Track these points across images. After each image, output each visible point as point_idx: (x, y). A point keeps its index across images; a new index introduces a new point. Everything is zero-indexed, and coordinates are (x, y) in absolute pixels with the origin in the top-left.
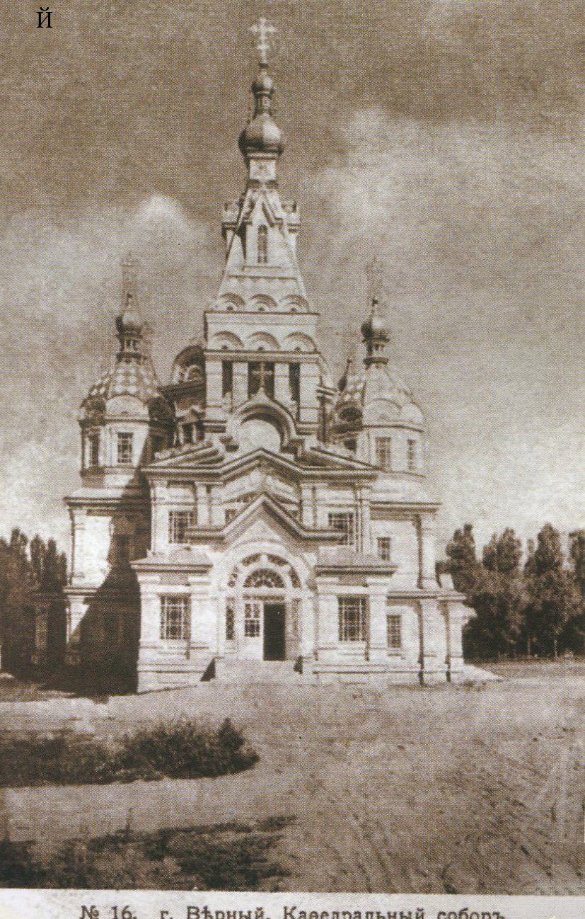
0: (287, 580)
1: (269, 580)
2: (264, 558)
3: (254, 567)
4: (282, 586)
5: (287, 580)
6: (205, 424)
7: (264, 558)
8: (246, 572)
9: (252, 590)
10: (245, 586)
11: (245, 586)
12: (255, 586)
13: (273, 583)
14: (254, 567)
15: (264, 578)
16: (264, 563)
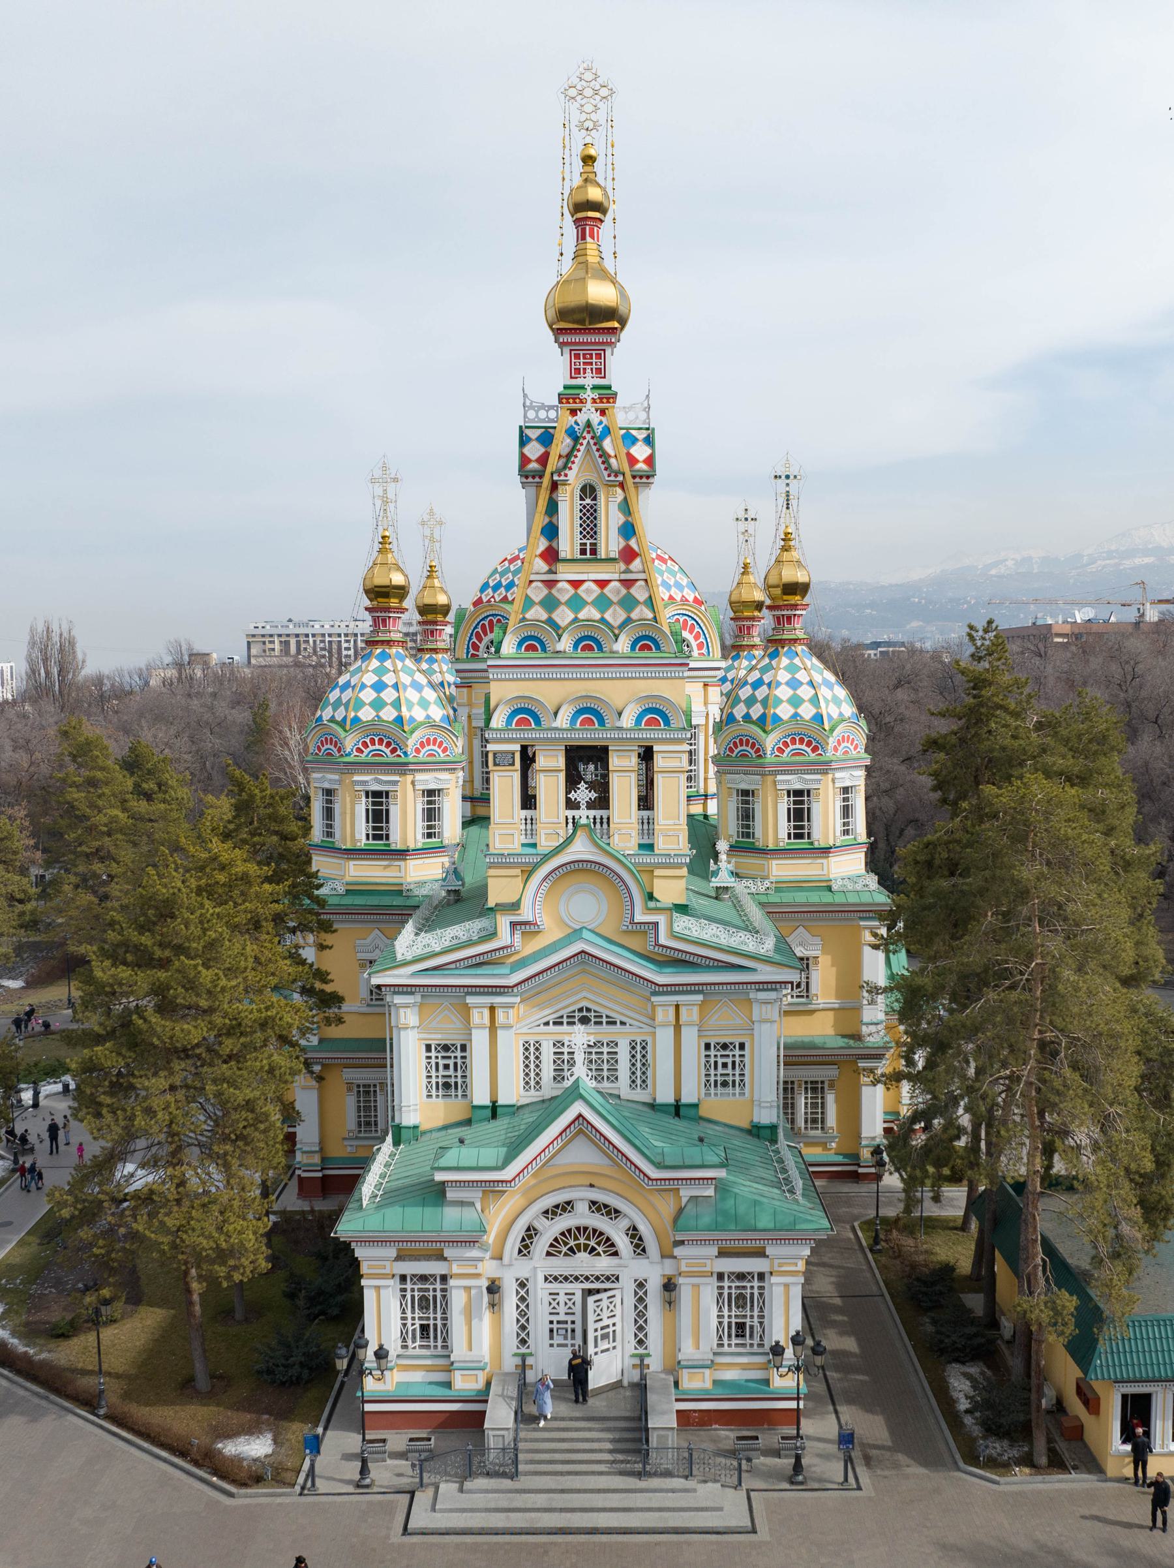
0: (623, 1243)
1: (592, 1243)
2: (582, 1208)
3: (564, 1222)
4: (616, 1254)
5: (623, 1243)
6: (368, 1407)
7: (582, 1208)
8: (551, 1229)
9: (560, 1265)
10: (548, 1254)
11: (548, 1254)
12: (566, 1254)
13: (600, 1249)
14: (564, 1222)
15: (582, 1241)
16: (582, 1216)
